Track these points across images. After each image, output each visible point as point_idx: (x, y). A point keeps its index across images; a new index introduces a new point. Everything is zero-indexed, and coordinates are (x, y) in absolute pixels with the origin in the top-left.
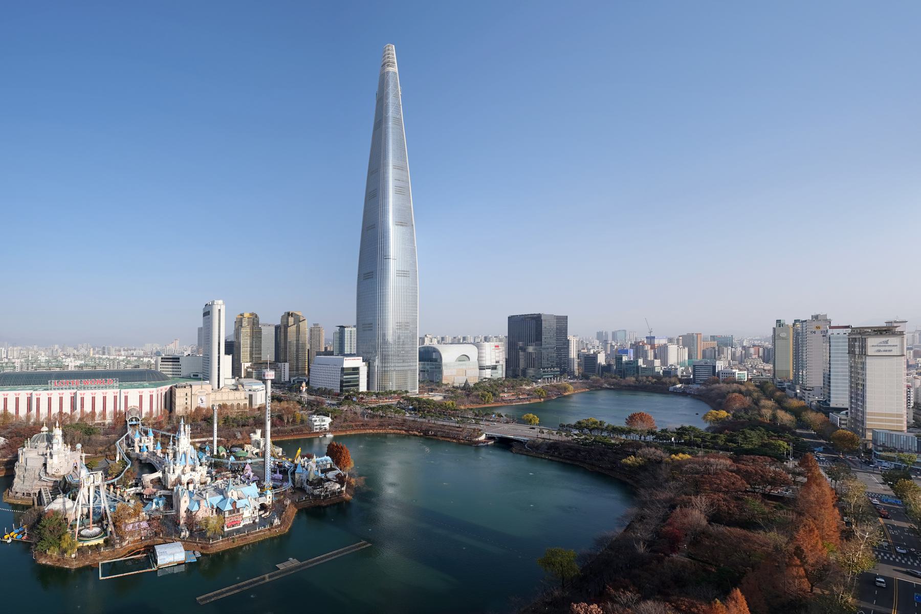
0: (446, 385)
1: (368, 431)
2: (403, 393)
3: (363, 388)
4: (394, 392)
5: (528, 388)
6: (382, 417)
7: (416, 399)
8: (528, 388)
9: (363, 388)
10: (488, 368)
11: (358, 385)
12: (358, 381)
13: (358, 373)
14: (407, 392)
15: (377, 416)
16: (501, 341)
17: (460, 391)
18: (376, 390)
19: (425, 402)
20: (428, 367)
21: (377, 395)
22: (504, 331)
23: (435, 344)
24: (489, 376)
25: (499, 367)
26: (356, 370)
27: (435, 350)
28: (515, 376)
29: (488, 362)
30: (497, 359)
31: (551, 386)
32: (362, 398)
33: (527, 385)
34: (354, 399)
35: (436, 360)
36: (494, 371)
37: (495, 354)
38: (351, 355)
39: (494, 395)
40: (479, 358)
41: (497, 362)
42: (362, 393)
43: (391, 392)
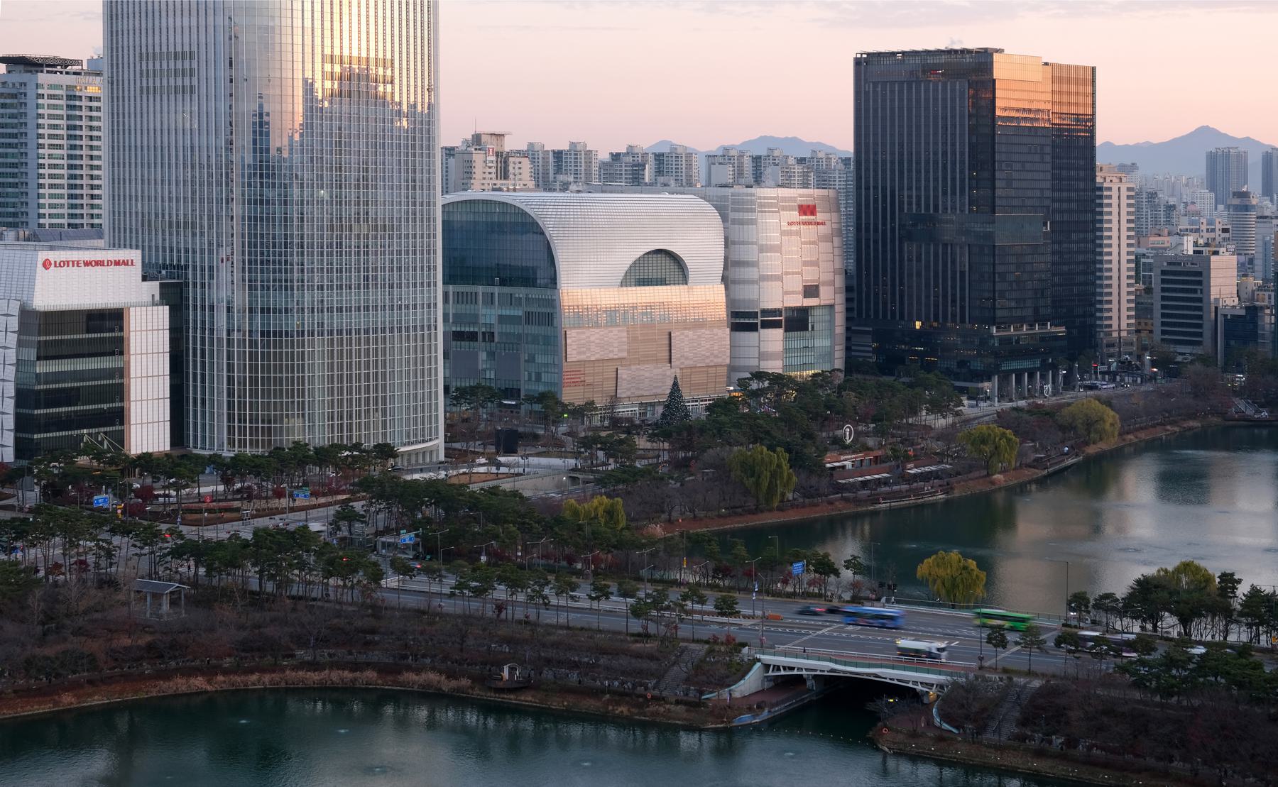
0: (580, 412)
1: (180, 685)
2: (363, 456)
3: (147, 431)
4: (324, 456)
5: (940, 422)
6: (256, 599)
7: (435, 492)
8: (940, 422)
9: (147, 431)
10: (770, 320)
11: (119, 416)
12: (119, 392)
13: (118, 347)
14: (385, 451)
15: (226, 594)
16: (823, 183)
17: (642, 443)
18: (218, 440)
19: (474, 502)
20: (488, 315)
21: (229, 470)
22: (839, 134)
23: (521, 193)
24: (775, 366)
25: (816, 319)
26: (105, 326)
27: (527, 227)
28: (890, 363)
29: (779, 295)
30: (811, 275)
31: (1035, 410)
32: (146, 494)
33: (937, 408)
34: (103, 499)
35: (526, 278)
36: (800, 339)
37: (798, 255)
38: (76, 229)
39: (797, 461)
40: (732, 271)
41: (811, 291)
42: (146, 461)
43: (300, 457)
